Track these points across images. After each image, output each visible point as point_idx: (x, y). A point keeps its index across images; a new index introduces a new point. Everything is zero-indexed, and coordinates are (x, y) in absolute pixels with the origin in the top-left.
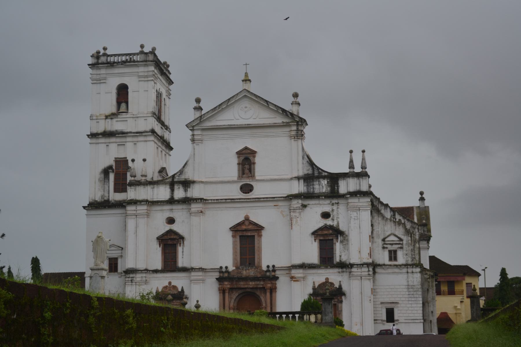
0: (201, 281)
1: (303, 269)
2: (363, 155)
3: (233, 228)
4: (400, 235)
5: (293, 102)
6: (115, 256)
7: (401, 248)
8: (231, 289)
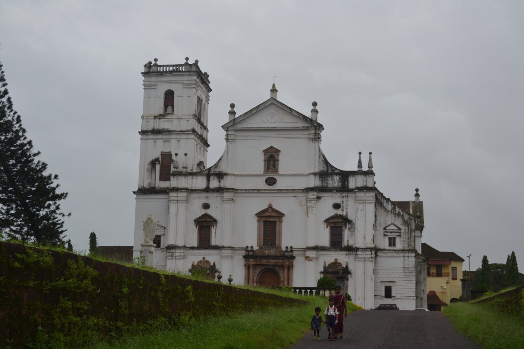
0: (230, 258)
1: (316, 251)
2: (370, 156)
4: (398, 225)
5: (312, 110)
6: (159, 234)
7: (400, 236)
8: (255, 266)
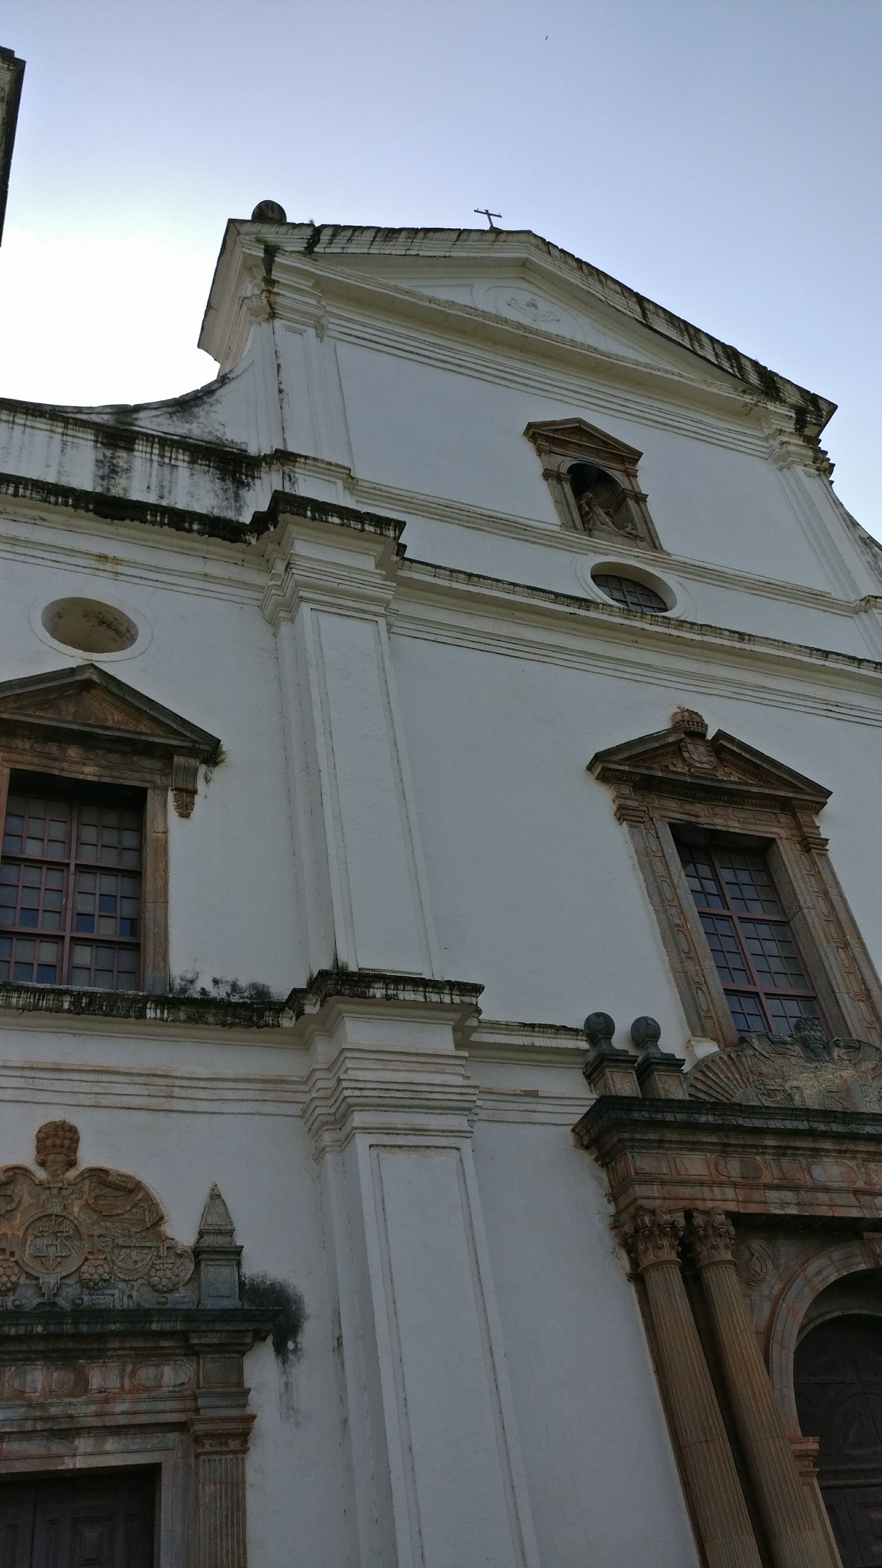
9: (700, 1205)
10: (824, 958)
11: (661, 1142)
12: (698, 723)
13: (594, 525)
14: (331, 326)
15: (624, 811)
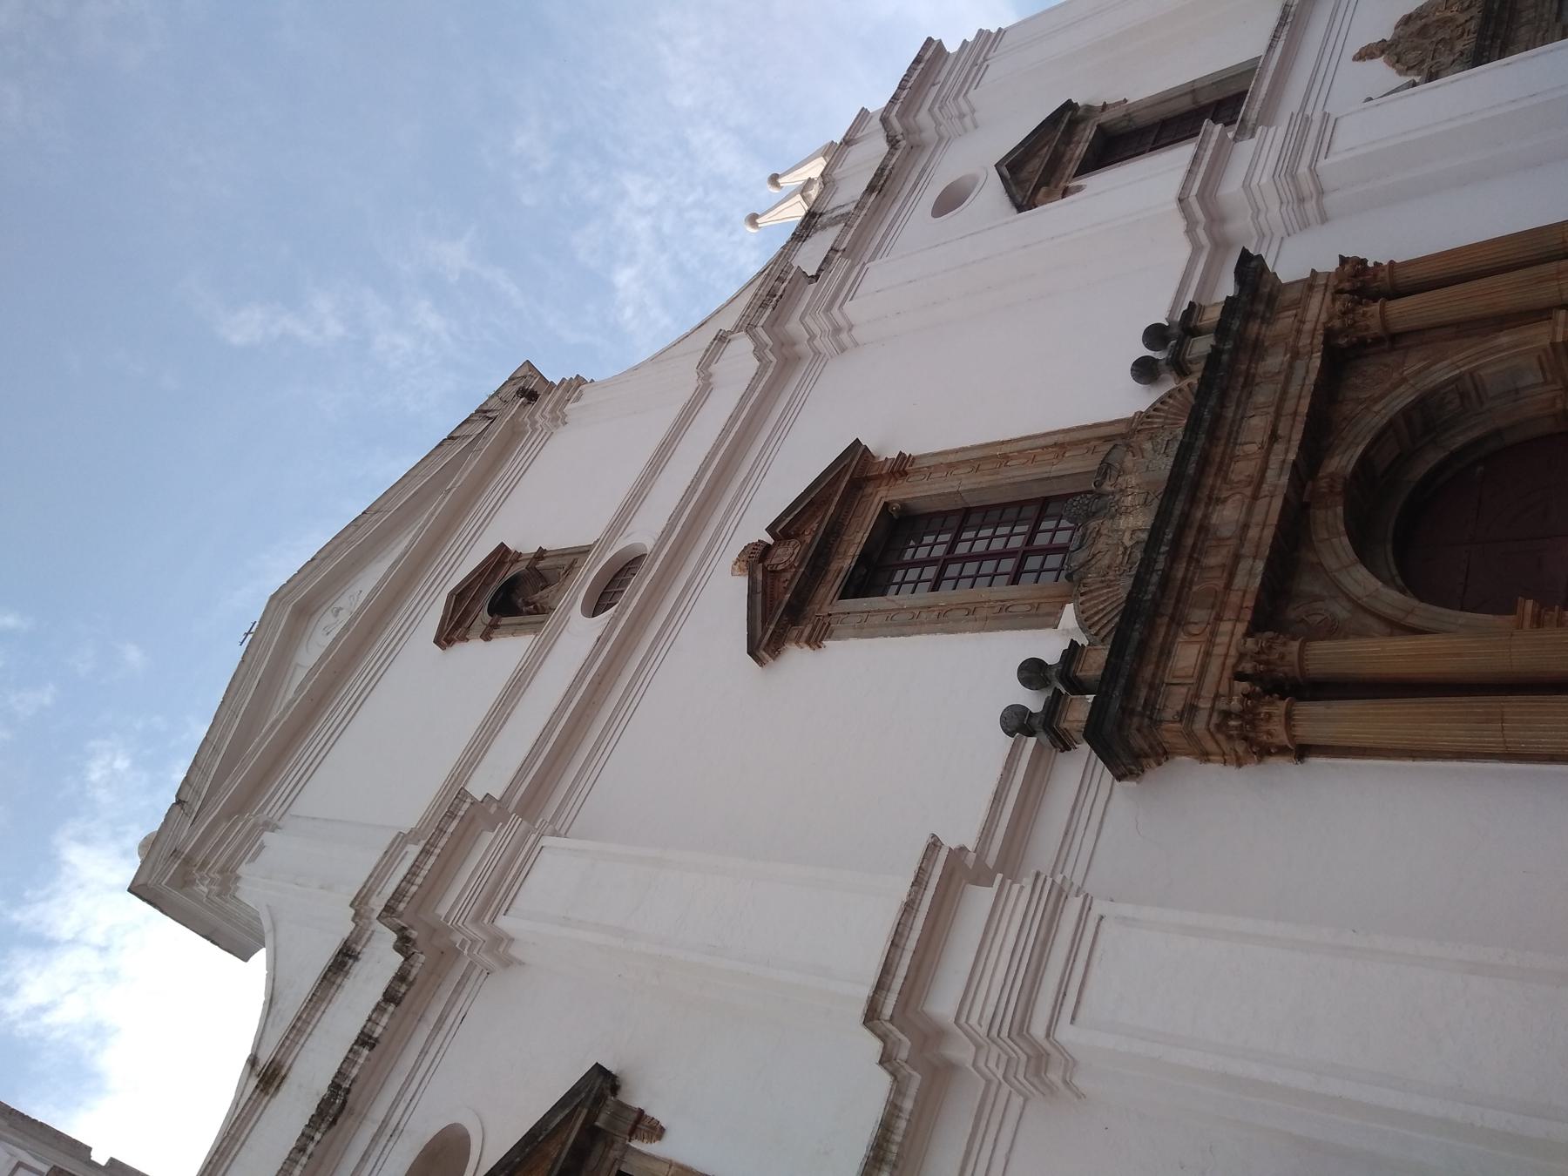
3: (759, 633)
9: (1231, 661)
10: (1012, 480)
11: (1151, 687)
12: (754, 549)
13: (547, 603)
14: (270, 816)
15: (813, 639)
